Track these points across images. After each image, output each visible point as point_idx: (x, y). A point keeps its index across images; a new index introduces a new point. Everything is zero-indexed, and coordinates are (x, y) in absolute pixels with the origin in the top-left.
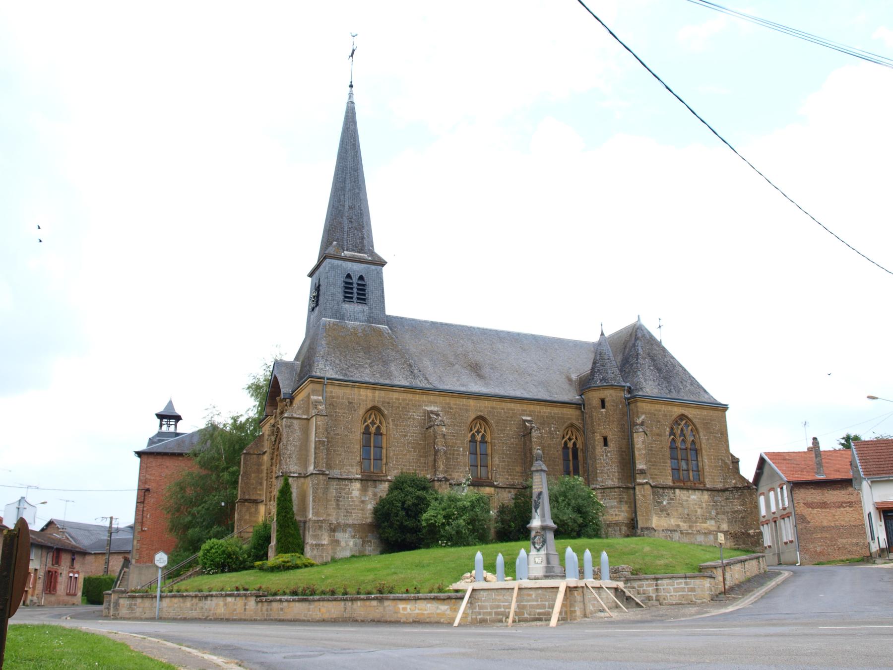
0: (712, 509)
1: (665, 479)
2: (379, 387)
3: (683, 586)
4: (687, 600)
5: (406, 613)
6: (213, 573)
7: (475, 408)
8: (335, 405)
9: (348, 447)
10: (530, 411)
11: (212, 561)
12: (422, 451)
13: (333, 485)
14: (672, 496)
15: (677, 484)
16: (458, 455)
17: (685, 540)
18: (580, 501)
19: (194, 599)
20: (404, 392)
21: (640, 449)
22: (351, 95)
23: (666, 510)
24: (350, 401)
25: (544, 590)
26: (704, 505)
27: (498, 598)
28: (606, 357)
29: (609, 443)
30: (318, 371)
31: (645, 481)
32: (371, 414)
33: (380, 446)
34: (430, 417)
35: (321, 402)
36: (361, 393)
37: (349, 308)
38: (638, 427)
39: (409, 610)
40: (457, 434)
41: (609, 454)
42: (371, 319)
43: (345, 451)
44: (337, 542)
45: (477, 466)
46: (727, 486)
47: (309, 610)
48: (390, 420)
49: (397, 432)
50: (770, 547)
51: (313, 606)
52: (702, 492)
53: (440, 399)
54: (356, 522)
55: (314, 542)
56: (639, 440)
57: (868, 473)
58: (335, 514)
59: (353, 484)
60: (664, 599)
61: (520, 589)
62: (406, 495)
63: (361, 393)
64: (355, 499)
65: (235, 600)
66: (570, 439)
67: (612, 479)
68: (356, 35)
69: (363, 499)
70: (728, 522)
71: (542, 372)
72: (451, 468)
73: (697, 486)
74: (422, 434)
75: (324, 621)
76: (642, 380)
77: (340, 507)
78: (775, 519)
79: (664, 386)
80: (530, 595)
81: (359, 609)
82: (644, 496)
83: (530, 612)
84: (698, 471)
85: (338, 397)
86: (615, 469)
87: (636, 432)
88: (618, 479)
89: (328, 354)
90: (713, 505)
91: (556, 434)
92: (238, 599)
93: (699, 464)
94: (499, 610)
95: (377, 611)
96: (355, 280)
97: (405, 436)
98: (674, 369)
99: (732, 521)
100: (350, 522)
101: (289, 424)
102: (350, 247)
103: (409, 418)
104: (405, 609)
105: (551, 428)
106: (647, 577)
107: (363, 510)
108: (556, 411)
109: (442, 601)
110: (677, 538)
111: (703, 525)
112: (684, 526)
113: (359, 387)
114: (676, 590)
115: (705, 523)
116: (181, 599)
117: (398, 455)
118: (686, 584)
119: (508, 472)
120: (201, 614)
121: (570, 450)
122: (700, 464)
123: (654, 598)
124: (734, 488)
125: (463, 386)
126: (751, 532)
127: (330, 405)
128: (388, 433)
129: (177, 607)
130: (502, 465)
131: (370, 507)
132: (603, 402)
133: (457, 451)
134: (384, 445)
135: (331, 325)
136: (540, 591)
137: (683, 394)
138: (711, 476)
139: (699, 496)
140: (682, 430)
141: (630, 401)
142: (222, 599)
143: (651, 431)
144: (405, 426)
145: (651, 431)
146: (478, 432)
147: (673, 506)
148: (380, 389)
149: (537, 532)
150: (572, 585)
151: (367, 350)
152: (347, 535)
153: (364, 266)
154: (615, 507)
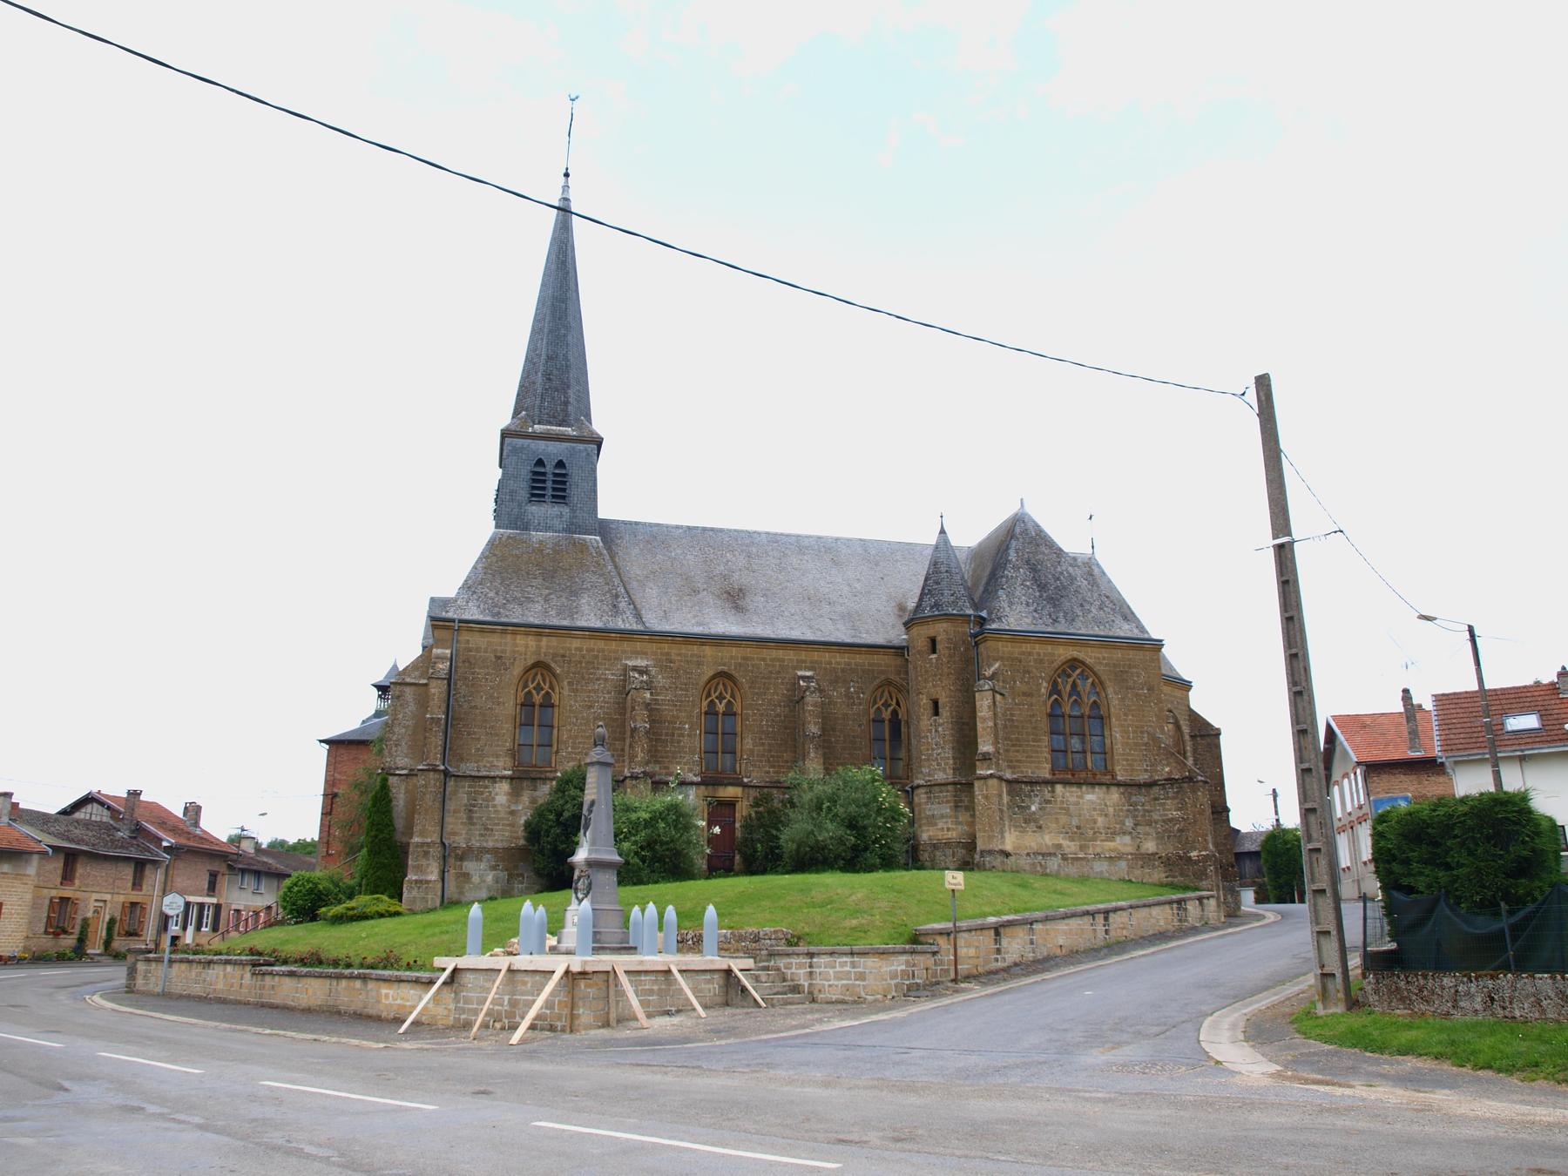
0: (1127, 817)
1: (1036, 767)
2: (547, 631)
3: (848, 969)
5: (387, 1002)
6: (296, 923)
8: (473, 661)
9: (492, 727)
11: (294, 904)
12: (618, 730)
14: (1048, 796)
16: (682, 735)
17: (1072, 870)
18: (853, 808)
20: (591, 638)
21: (984, 720)
22: (566, 187)
23: (1035, 821)
24: (499, 654)
26: (1111, 810)
28: (943, 569)
29: (940, 710)
31: (989, 772)
32: (536, 674)
33: (550, 724)
35: (446, 658)
36: (518, 641)
37: (537, 511)
38: (981, 682)
40: (681, 701)
41: (940, 729)
44: (466, 876)
45: (717, 753)
46: (1157, 778)
48: (565, 683)
49: (576, 701)
50: (1348, 868)
54: (499, 845)
56: (983, 703)
57: (1449, 748)
58: (464, 832)
59: (497, 785)
60: (820, 991)
61: (510, 970)
62: (567, 802)
63: (518, 641)
64: (500, 809)
68: (577, 98)
69: (513, 808)
70: (1157, 838)
71: (855, 598)
72: (667, 758)
73: (1101, 778)
74: (618, 703)
76: (1005, 605)
77: (475, 821)
78: (1352, 824)
79: (1045, 612)
80: (525, 983)
82: (986, 797)
84: (1105, 753)
85: (478, 650)
86: (948, 753)
87: (979, 691)
88: (954, 769)
89: (481, 584)
90: (1128, 810)
91: (859, 698)
92: (237, 967)
97: (590, 707)
98: (1072, 583)
99: (1163, 837)
100: (490, 844)
103: (598, 679)
104: (387, 996)
105: (849, 688)
106: (797, 952)
107: (512, 825)
108: (860, 659)
110: (1056, 867)
111: (1109, 843)
112: (1070, 846)
113: (514, 633)
115: (1111, 841)
117: (576, 737)
118: (853, 965)
121: (886, 722)
122: (1108, 742)
123: (806, 990)
125: (699, 624)
126: (1194, 854)
127: (464, 662)
128: (562, 703)
130: (759, 750)
132: (933, 641)
134: (556, 724)
135: (504, 539)
137: (1080, 624)
138: (1127, 760)
139: (1102, 795)
140: (1074, 685)
142: (221, 967)
143: (1012, 688)
144: (590, 692)
145: (1012, 688)
146: (721, 698)
147: (1049, 814)
148: (549, 635)
150: (576, 968)
151: (549, 576)
152: (483, 865)
154: (947, 817)
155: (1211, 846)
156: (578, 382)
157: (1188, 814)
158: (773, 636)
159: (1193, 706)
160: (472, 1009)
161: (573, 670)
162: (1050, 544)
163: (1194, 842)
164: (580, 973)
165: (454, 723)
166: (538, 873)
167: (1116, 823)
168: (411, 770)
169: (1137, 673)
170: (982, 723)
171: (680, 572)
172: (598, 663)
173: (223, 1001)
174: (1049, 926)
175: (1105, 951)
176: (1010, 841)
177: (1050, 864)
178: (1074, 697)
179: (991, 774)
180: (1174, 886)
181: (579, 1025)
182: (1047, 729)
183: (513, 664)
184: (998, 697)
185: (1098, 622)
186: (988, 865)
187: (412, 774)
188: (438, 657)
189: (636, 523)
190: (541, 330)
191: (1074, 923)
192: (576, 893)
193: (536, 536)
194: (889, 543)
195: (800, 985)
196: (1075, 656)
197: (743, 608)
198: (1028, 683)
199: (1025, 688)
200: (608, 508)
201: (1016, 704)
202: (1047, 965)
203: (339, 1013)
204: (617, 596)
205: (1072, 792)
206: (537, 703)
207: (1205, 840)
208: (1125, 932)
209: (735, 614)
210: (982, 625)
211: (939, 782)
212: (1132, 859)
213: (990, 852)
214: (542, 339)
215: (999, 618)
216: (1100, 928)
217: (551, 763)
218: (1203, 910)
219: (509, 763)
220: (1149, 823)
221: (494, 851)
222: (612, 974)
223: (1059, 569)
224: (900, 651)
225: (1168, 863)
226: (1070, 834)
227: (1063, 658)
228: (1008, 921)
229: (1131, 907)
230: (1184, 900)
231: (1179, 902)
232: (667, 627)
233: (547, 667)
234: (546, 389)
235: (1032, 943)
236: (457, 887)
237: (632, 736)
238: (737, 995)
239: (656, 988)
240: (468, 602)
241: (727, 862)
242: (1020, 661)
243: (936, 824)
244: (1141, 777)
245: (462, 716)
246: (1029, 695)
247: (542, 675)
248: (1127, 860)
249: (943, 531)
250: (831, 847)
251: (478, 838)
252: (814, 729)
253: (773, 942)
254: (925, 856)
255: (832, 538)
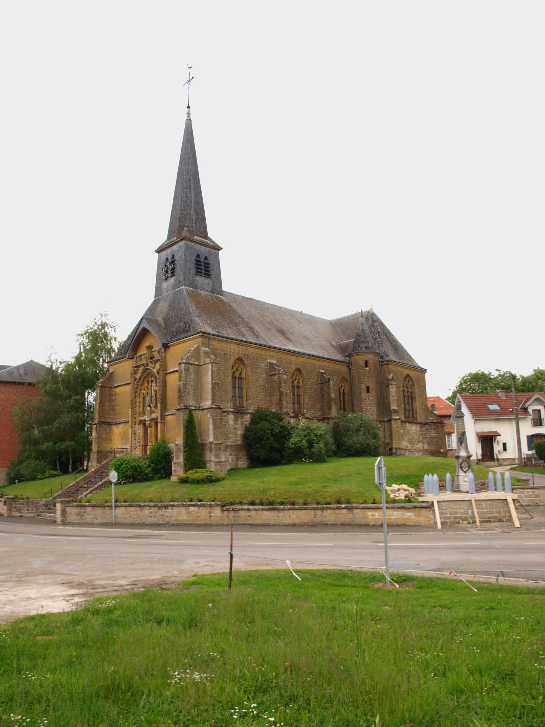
2: (243, 343)
3: (531, 494)
4: (532, 503)
5: (374, 518)
9: (225, 388)
10: (324, 366)
19: (153, 509)
21: (393, 396)
26: (418, 433)
27: (456, 507)
29: (370, 391)
31: (398, 417)
34: (274, 368)
41: (371, 398)
43: (224, 391)
47: (278, 517)
51: (281, 514)
53: (276, 354)
54: (232, 444)
55: (217, 460)
59: (229, 415)
64: (231, 427)
65: (199, 509)
66: (341, 387)
69: (235, 426)
70: (428, 444)
74: (266, 379)
75: (294, 525)
81: (329, 516)
82: (397, 427)
83: (482, 516)
85: (218, 349)
86: (374, 408)
88: (377, 415)
92: (201, 508)
94: (457, 515)
95: (347, 517)
97: (258, 380)
99: (430, 444)
101: (187, 368)
103: (259, 368)
107: (235, 435)
109: (407, 510)
112: (410, 446)
114: (526, 497)
116: (138, 509)
117: (254, 394)
118: (533, 492)
119: (313, 408)
120: (161, 520)
122: (414, 407)
124: (432, 422)
126: (442, 450)
129: (133, 514)
131: (240, 432)
136: (489, 502)
142: (184, 508)
152: (227, 453)
153: (208, 249)
163: (441, 446)
168: (195, 407)
173: (185, 524)
183: (230, 357)
186: (398, 454)
203: (327, 524)
214: (190, 192)
219: (232, 406)
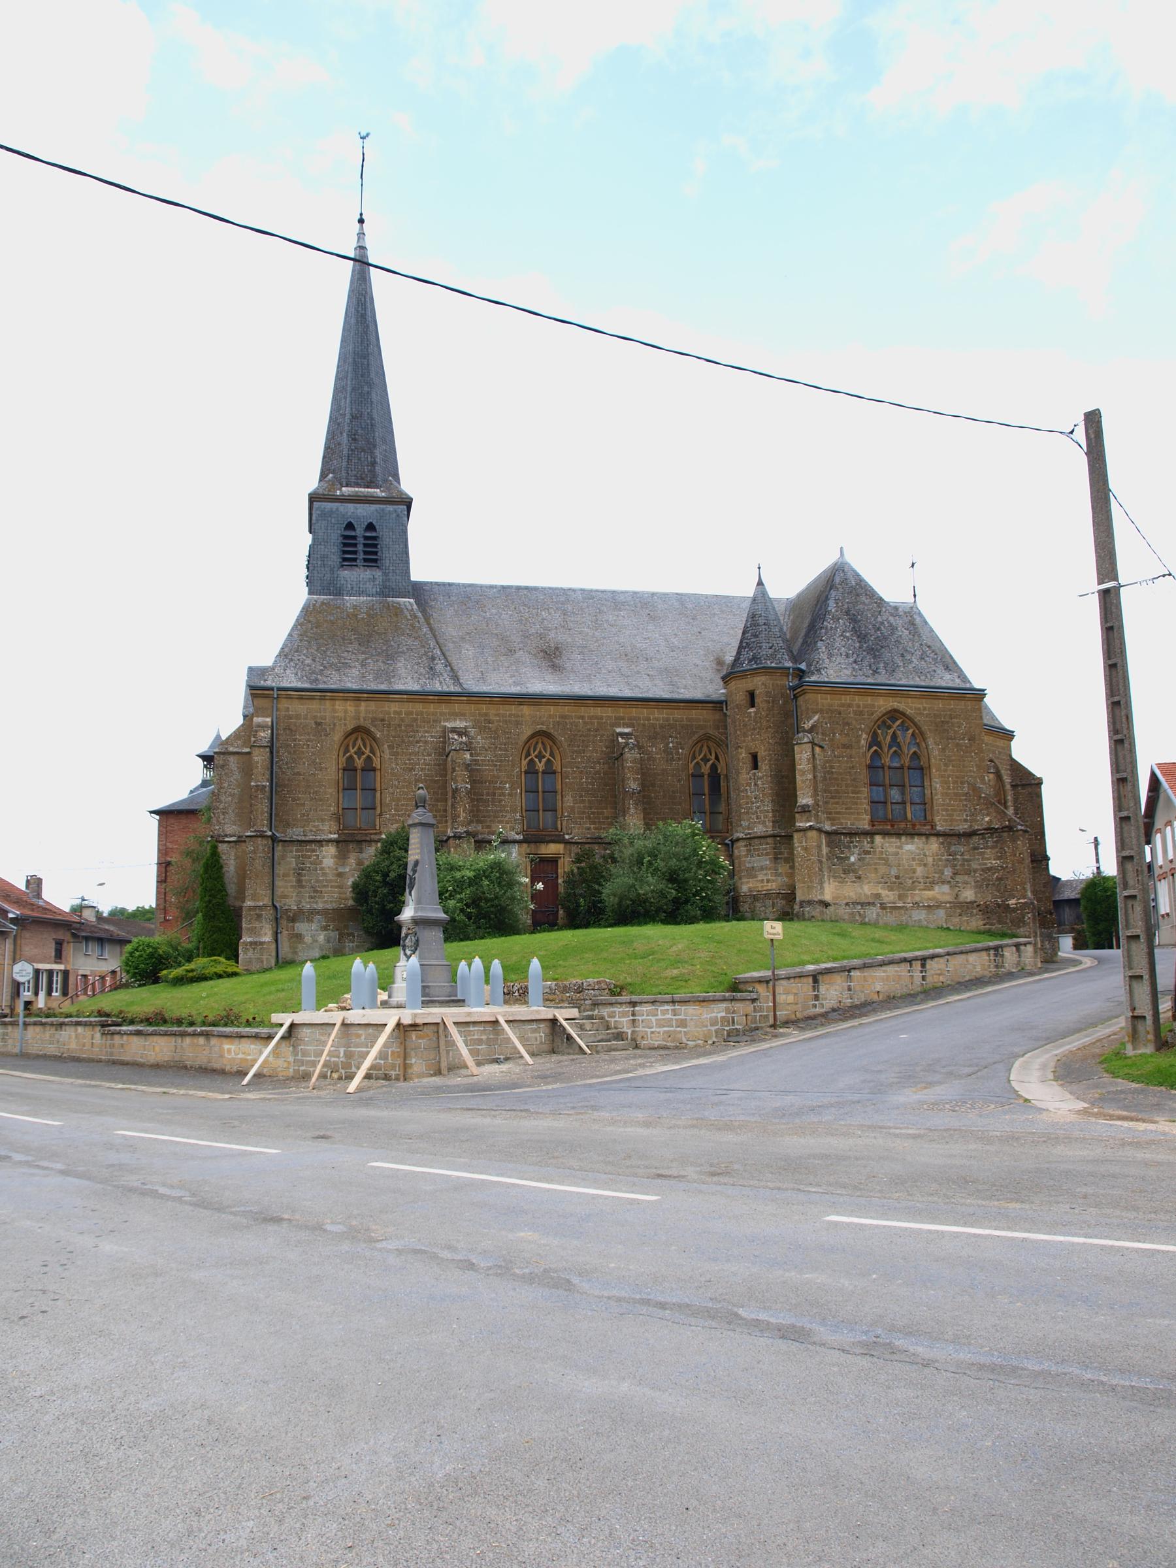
1: (855, 819)
2: (365, 695)
3: (669, 1016)
4: (673, 1041)
6: (140, 986)
7: (530, 719)
8: (294, 728)
10: (630, 719)
11: (136, 969)
13: (292, 852)
14: (867, 847)
15: (878, 827)
16: (503, 794)
17: (890, 918)
18: (673, 862)
21: (803, 773)
22: (361, 235)
23: (854, 871)
25: (375, 1028)
26: (930, 860)
28: (761, 621)
29: (759, 764)
30: (270, 677)
31: (808, 824)
35: (266, 726)
36: (337, 707)
37: (349, 576)
38: (801, 735)
39: (233, 1054)
40: (501, 761)
42: (386, 591)
43: (312, 799)
44: (299, 937)
45: (538, 811)
46: (976, 828)
48: (386, 746)
49: (397, 764)
50: (1167, 914)
52: (927, 838)
54: (329, 906)
56: (802, 756)
61: (344, 1024)
62: (392, 863)
63: (337, 707)
67: (764, 823)
68: (368, 135)
69: (340, 870)
70: (976, 887)
71: (672, 654)
73: (921, 828)
74: (439, 765)
76: (824, 656)
77: (304, 883)
78: (1173, 871)
79: (866, 663)
82: (806, 849)
84: (925, 804)
85: (298, 717)
88: (773, 822)
89: (297, 651)
91: (678, 753)
93: (926, 792)
96: (360, 531)
97: (411, 770)
98: (892, 634)
99: (981, 886)
100: (320, 906)
102: (353, 479)
103: (418, 742)
104: (229, 1051)
106: (620, 1001)
107: (340, 887)
108: (677, 714)
110: (874, 916)
111: (927, 892)
112: (888, 896)
113: (333, 699)
115: (930, 890)
117: (399, 799)
118: (675, 1013)
119: (590, 818)
122: (928, 792)
125: (516, 684)
126: (1012, 902)
127: (284, 729)
128: (383, 766)
130: (579, 807)
132: (752, 695)
133: (500, 788)
135: (317, 606)
138: (947, 810)
139: (921, 846)
140: (894, 736)
141: (795, 692)
143: (832, 740)
144: (410, 755)
145: (832, 740)
147: (868, 864)
148: (367, 700)
149: (409, 929)
150: (407, 1021)
151: (365, 641)
152: (314, 926)
153: (374, 507)
154: (766, 869)
155: (1029, 894)
156: (384, 441)
157: (1007, 863)
158: (590, 693)
159: (1016, 755)
160: (310, 1061)
161: (393, 733)
162: (871, 594)
164: (411, 1025)
165: (279, 789)
166: (368, 932)
167: (935, 873)
168: (239, 837)
169: (958, 722)
170: (801, 776)
171: (495, 632)
172: (417, 725)
174: (867, 973)
175: (922, 996)
176: (829, 891)
177: (868, 912)
178: (894, 749)
179: (810, 826)
180: (990, 933)
181: (412, 1074)
182: (867, 781)
184: (817, 749)
185: (920, 673)
186: (807, 916)
187: (240, 841)
188: (259, 726)
189: (450, 585)
190: (344, 388)
191: (891, 970)
192: (404, 950)
193: (350, 601)
194: (706, 596)
195: (623, 1032)
196: (895, 707)
197: (560, 667)
198: (847, 735)
199: (845, 740)
200: (419, 572)
201: (835, 756)
202: (864, 1010)
203: (185, 1067)
204: (433, 658)
205: (892, 842)
206: (359, 767)
207: (1024, 888)
208: (941, 979)
209: (552, 673)
210: (801, 678)
211: (759, 834)
212: (951, 908)
213: (810, 903)
214: (345, 398)
215: (819, 671)
216: (917, 975)
217: (375, 826)
218: (1020, 956)
219: (335, 828)
220: (968, 872)
221: (324, 912)
222: (442, 1025)
223: (879, 619)
224: (718, 705)
225: (986, 911)
226: (889, 884)
227: (883, 710)
228: (826, 969)
229: (948, 954)
230: (1002, 947)
231: (996, 948)
232: (485, 689)
233: (367, 732)
234: (352, 450)
235: (849, 989)
236: (290, 947)
237: (454, 797)
238: (563, 1042)
239: (484, 1037)
240: (285, 670)
241: (551, 917)
242: (840, 714)
243: (756, 876)
244: (961, 827)
245: (286, 782)
246: (848, 748)
247: (363, 740)
248: (945, 908)
249: (760, 583)
250: (652, 900)
251: (308, 900)
252: (633, 785)
253: (597, 992)
254: (745, 908)
255: (648, 593)
